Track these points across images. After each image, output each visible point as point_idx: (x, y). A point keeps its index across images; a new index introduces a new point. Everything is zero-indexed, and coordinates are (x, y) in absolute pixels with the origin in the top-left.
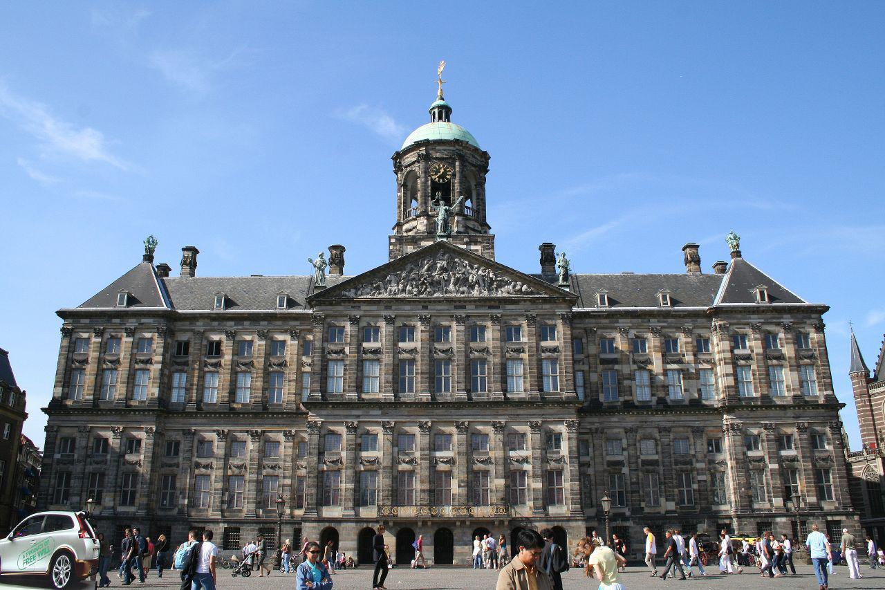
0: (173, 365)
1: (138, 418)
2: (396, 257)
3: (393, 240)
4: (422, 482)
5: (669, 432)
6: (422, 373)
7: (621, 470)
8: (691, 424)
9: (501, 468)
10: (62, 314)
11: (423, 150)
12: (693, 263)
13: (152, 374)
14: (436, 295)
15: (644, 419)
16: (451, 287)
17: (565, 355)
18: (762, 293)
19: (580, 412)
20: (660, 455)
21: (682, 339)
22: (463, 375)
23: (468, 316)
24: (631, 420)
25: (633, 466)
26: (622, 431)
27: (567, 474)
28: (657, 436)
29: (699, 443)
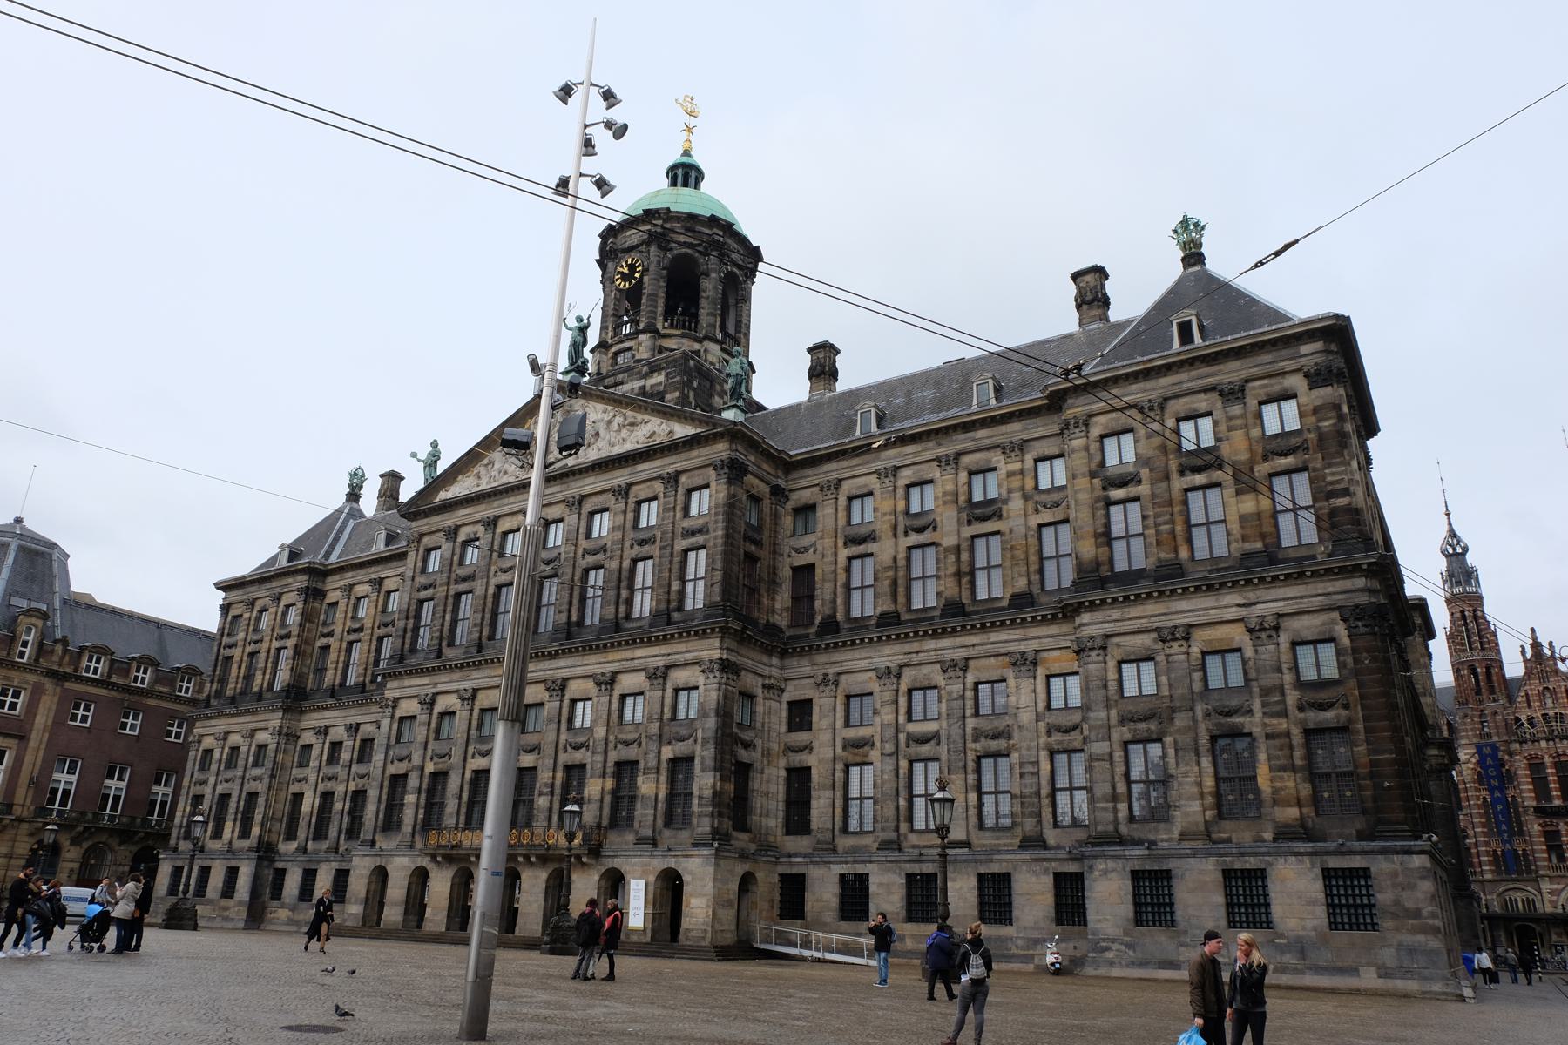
1: (267, 716)
5: (965, 669)
7: (866, 755)
8: (1014, 648)
9: (600, 758)
10: (221, 586)
12: (1085, 307)
15: (915, 646)
18: (1185, 329)
20: (944, 724)
23: (583, 497)
24: (889, 655)
25: (889, 748)
26: (873, 674)
28: (940, 679)
29: (1026, 684)
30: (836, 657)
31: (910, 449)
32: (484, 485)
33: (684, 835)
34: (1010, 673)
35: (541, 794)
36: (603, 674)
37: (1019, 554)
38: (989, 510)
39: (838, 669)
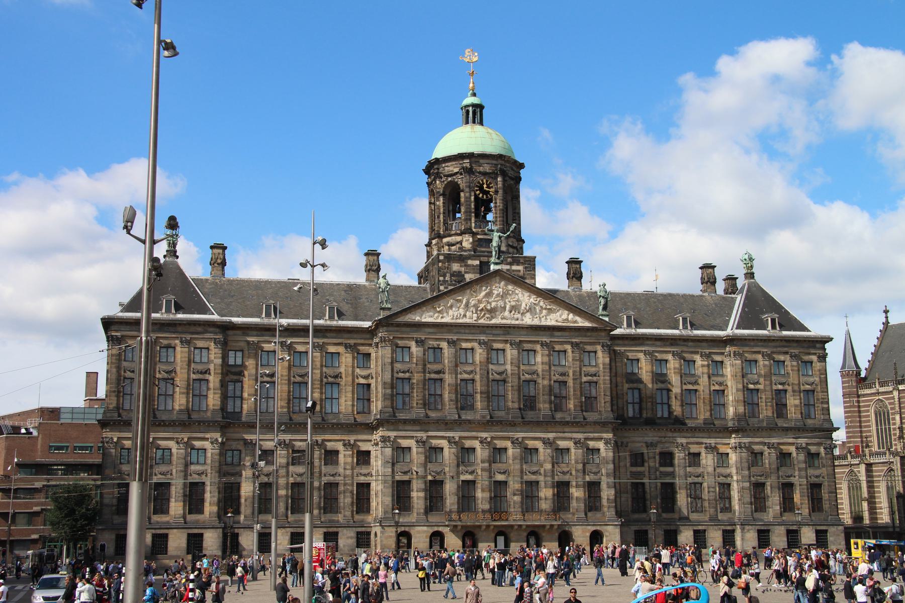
0: (227, 375)
2: (444, 276)
3: (441, 258)
4: (483, 491)
6: (481, 393)
9: (549, 479)
11: (466, 163)
13: (211, 385)
14: (494, 321)
15: (663, 434)
16: (507, 313)
17: (604, 380)
18: (773, 321)
19: (615, 431)
21: (699, 361)
22: (516, 396)
24: (651, 436)
26: (644, 445)
27: (604, 486)
29: (710, 456)
30: (626, 434)
31: (658, 343)
32: (447, 319)
33: (598, 515)
34: (703, 451)
35: (515, 495)
36: (549, 439)
37: (707, 402)
38: (693, 380)
39: (627, 440)
